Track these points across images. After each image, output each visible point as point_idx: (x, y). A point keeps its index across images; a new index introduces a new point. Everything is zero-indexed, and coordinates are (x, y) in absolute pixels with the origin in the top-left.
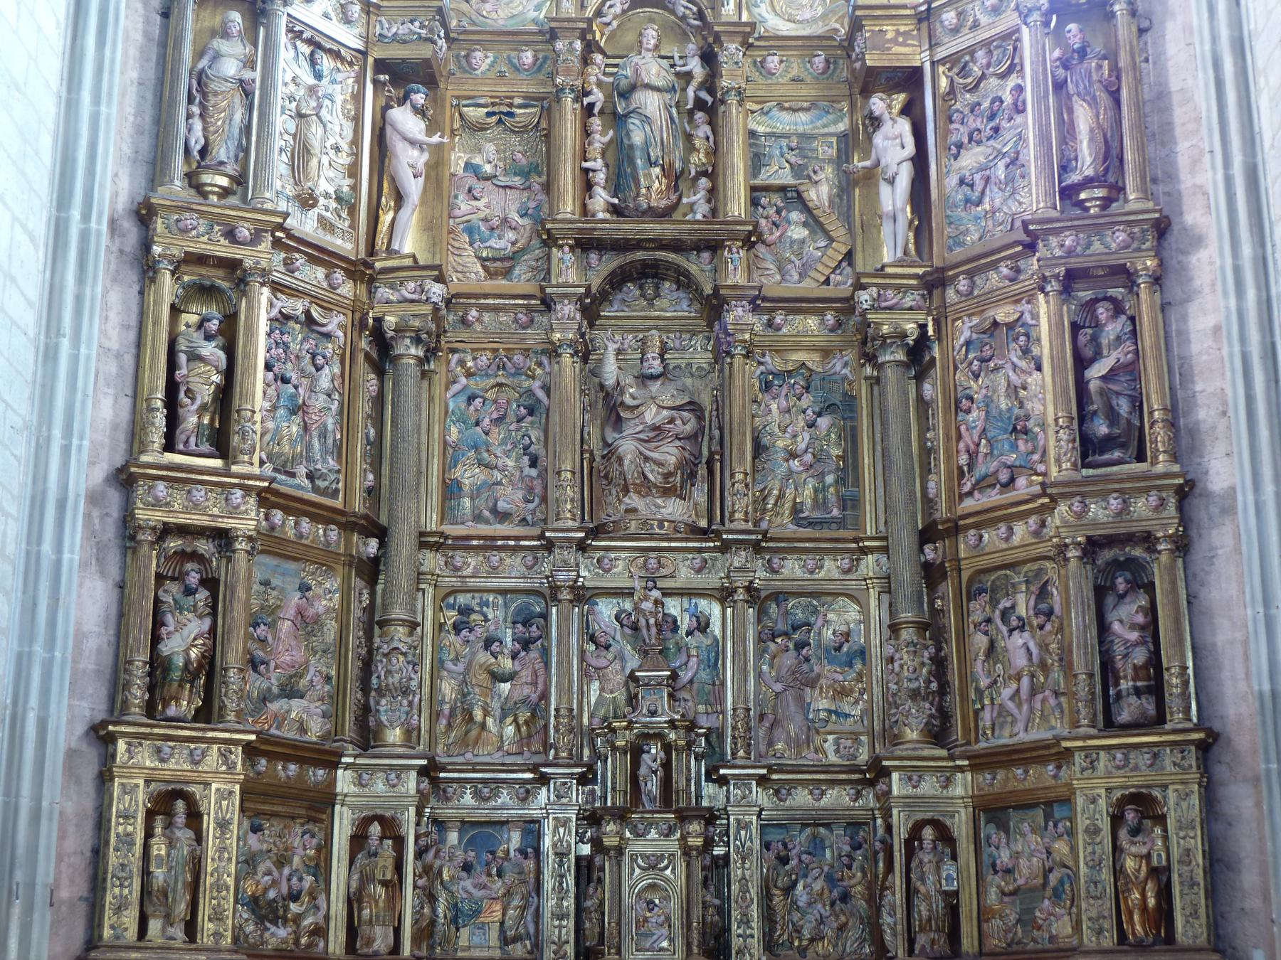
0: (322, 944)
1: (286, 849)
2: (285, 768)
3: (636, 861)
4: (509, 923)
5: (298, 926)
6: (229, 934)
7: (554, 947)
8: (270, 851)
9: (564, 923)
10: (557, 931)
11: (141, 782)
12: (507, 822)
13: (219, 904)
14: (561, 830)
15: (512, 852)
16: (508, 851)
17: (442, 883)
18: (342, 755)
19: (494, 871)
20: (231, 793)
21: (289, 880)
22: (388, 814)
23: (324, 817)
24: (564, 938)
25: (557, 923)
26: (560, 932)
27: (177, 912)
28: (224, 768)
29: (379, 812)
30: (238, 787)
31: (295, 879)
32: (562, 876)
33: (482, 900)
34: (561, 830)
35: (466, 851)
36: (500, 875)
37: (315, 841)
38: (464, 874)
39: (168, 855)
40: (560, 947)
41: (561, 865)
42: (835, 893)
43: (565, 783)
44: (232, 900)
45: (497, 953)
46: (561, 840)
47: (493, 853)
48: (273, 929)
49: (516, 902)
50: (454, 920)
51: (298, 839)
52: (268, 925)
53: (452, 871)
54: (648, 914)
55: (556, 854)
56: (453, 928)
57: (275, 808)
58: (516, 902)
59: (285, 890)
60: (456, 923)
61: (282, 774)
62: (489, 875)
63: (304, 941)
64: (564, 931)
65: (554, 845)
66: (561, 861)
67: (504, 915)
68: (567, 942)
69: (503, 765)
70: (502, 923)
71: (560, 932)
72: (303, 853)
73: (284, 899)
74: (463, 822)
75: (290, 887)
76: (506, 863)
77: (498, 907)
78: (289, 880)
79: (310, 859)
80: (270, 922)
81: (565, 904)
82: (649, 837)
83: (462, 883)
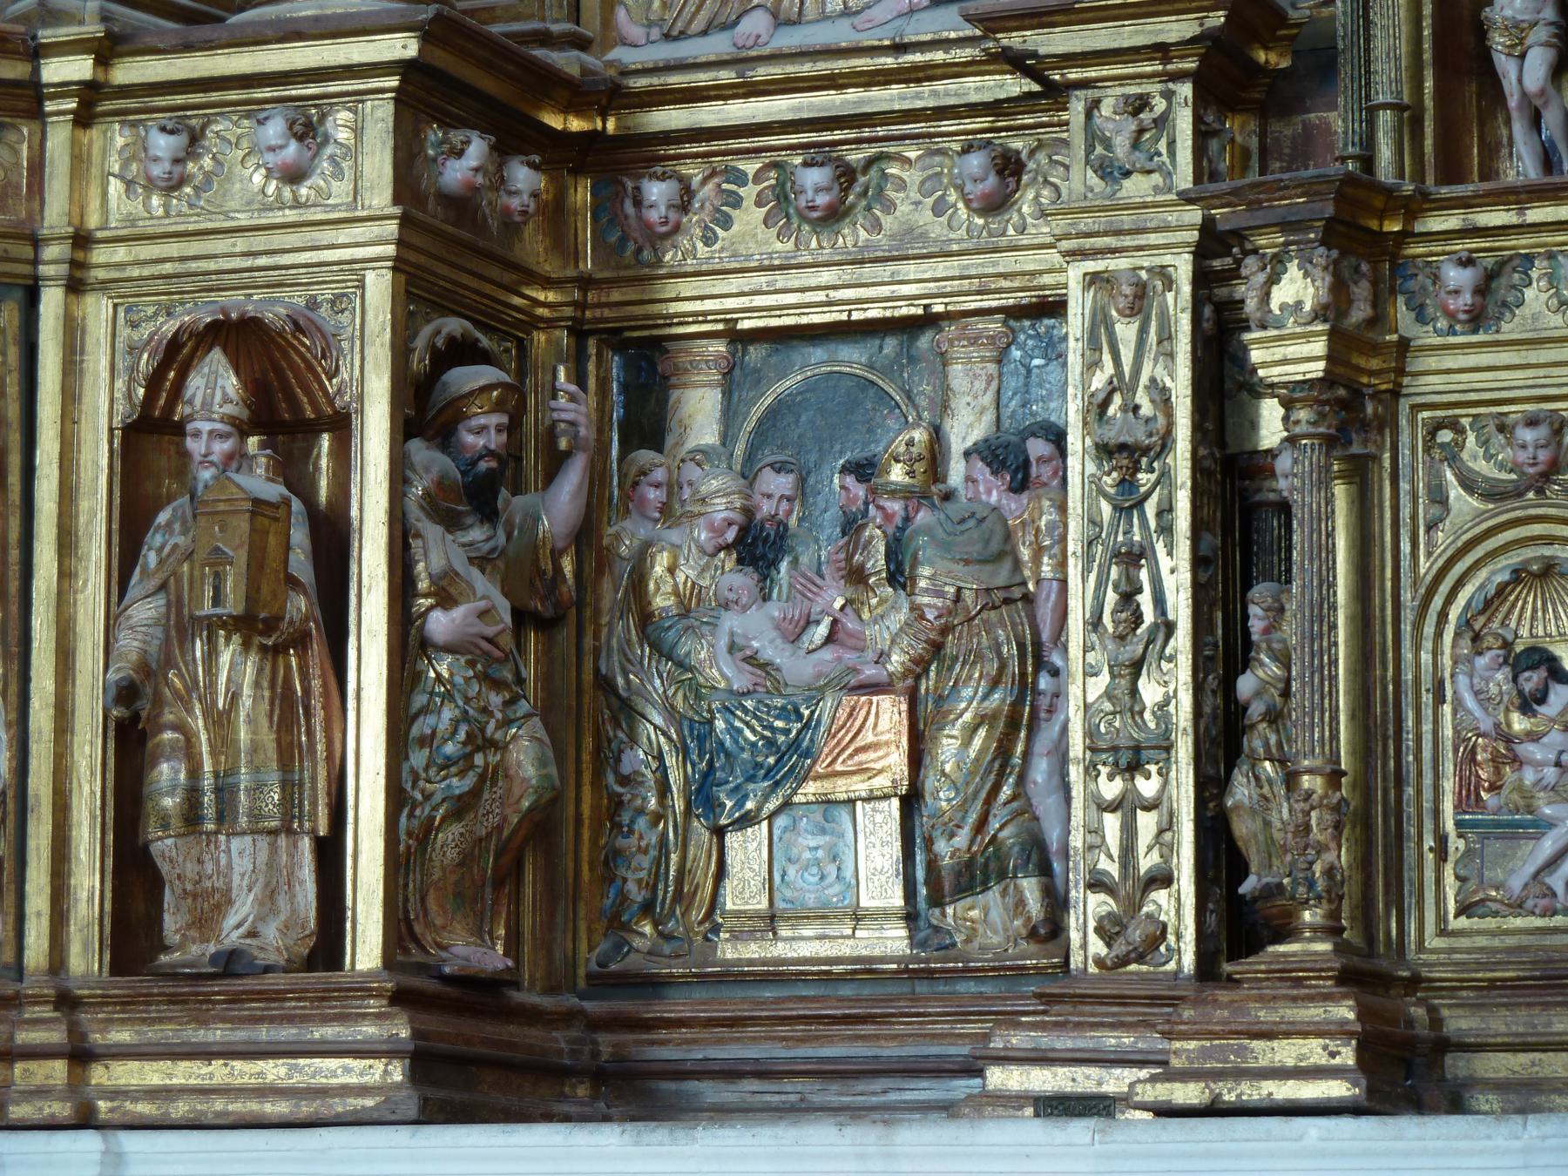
3: (1452, 456)
4: (941, 797)
7: (1099, 904)
9: (1148, 787)
10: (1112, 824)
12: (929, 321)
14: (1126, 332)
15: (956, 472)
16: (934, 458)
17: (646, 618)
18: (37, 53)
19: (877, 561)
22: (274, 308)
24: (1147, 861)
25: (1111, 789)
26: (1129, 831)
29: (236, 302)
32: (1133, 557)
33: (815, 694)
34: (1126, 332)
35: (749, 475)
36: (899, 575)
38: (741, 581)
40: (1133, 905)
41: (1129, 502)
43: (1139, 105)
45: (892, 941)
46: (1119, 385)
47: (864, 470)
49: (971, 699)
50: (702, 796)
53: (686, 573)
54: (1519, 723)
55: (1105, 451)
56: (701, 832)
58: (971, 699)
60: (712, 806)
62: (856, 576)
64: (1147, 823)
65: (1098, 408)
66: (1127, 483)
67: (917, 757)
68: (1162, 878)
69: (899, 48)
70: (911, 801)
71: (1129, 831)
74: (738, 338)
76: (923, 517)
77: (889, 715)
81: (1150, 692)
82: (1510, 329)
83: (731, 622)
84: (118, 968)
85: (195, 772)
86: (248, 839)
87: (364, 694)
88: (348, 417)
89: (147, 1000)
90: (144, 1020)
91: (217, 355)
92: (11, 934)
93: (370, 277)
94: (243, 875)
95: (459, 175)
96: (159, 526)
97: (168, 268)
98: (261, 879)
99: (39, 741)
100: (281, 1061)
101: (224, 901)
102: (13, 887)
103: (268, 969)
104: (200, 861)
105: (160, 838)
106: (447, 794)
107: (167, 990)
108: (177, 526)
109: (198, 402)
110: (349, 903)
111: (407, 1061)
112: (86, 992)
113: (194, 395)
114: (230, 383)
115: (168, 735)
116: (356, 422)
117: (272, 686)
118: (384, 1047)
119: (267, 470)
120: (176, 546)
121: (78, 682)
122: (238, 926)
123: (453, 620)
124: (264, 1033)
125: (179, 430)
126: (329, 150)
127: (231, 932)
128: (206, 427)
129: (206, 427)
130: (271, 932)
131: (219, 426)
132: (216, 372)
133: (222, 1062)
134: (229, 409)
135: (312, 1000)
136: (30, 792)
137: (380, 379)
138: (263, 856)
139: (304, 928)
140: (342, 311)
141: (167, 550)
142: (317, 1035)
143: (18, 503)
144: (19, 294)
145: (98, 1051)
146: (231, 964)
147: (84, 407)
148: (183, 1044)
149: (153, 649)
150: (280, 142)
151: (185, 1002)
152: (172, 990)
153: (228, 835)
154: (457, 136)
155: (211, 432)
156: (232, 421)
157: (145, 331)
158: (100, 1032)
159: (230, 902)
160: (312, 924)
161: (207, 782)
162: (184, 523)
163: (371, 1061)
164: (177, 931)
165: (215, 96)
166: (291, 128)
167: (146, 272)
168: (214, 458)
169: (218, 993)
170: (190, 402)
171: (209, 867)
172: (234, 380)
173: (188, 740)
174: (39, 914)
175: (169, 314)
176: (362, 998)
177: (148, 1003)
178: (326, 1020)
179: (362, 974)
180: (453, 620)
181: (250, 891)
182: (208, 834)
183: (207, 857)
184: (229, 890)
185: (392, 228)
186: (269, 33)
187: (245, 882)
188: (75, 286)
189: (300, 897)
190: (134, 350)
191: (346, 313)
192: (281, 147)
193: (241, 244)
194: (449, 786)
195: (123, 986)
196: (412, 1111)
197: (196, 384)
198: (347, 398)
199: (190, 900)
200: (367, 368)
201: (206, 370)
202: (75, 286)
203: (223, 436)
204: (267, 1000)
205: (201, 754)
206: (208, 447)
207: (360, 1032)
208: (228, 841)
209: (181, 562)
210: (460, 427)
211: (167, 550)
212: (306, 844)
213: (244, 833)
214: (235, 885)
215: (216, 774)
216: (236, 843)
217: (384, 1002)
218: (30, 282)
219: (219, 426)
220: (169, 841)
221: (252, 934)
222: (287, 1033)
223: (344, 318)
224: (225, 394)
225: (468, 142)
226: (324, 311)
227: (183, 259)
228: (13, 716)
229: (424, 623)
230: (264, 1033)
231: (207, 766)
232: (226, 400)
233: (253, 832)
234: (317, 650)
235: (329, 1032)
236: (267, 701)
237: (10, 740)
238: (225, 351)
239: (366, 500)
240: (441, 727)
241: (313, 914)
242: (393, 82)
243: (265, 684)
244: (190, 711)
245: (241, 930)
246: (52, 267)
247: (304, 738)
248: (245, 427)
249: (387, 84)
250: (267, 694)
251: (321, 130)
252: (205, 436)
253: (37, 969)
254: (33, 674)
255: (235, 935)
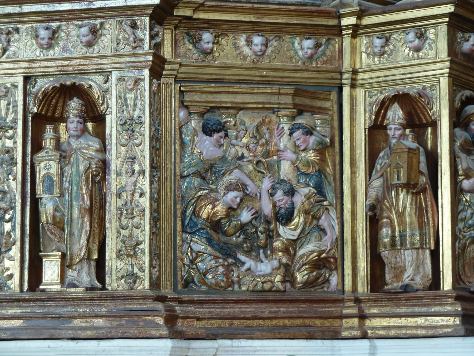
0: (334, 280)
1: (267, 154)
2: (249, 42)
5: (292, 257)
6: (146, 274)
8: (242, 157)
11: (20, 81)
13: (131, 236)
18: (340, 17)
20: (137, 81)
21: (272, 195)
22: (412, 90)
23: (327, 104)
27: (76, 248)
28: (128, 50)
29: (401, 89)
30: (146, 73)
31: (279, 195)
37: (312, 140)
39: (61, 174)
42: (11, 29)
44: (147, 228)
48: (249, 263)
51: (285, 138)
52: (243, 258)
57: (239, 99)
59: (267, 209)
61: (247, 50)
63: (300, 277)
72: (294, 157)
73: (268, 222)
75: (274, 205)
78: (272, 195)
79: (308, 164)
80: (248, 253)
84: (372, 290)
85: (393, 231)
86: (410, 251)
87: (444, 206)
88: (436, 122)
89: (382, 300)
90: (381, 306)
91: (396, 105)
92: (340, 281)
93: (442, 79)
94: (409, 262)
95: (468, 47)
96: (380, 157)
97: (381, 79)
98: (415, 263)
99: (347, 223)
100: (422, 318)
101: (404, 270)
102: (340, 267)
103: (417, 290)
104: (396, 258)
105: (384, 251)
106: (470, 236)
107: (387, 297)
108: (386, 157)
109: (391, 119)
110: (441, 269)
111: (461, 317)
112: (363, 298)
113: (389, 117)
114: (400, 113)
115: (385, 220)
116: (438, 123)
117: (416, 205)
118: (453, 313)
119: (412, 139)
120: (385, 163)
121: (358, 205)
122: (408, 277)
123: (470, 183)
124: (417, 310)
125: (385, 128)
126: (428, 41)
127: (406, 279)
128: (393, 127)
129: (393, 127)
130: (418, 279)
131: (397, 126)
132: (396, 110)
133: (404, 318)
134: (400, 121)
135: (431, 299)
136: (345, 238)
137: (445, 110)
138: (415, 256)
139: (428, 278)
140: (433, 90)
141: (383, 164)
142: (433, 310)
143: (338, 151)
144: (336, 89)
145: (368, 315)
146: (406, 289)
147: (357, 122)
148: (393, 313)
149: (380, 194)
150: (413, 40)
151: (393, 300)
152: (389, 297)
153: (404, 250)
154: (467, 35)
155: (395, 128)
156: (401, 124)
157: (374, 99)
158: (368, 310)
159: (405, 270)
160: (430, 276)
161: (397, 234)
162: (388, 156)
163: (450, 318)
164: (390, 279)
165: (393, 27)
166: (416, 35)
167: (374, 81)
168: (396, 136)
169: (403, 298)
170: (388, 119)
171: (399, 260)
172: (401, 112)
173: (391, 221)
174: (348, 275)
175: (381, 93)
176: (446, 298)
177: (382, 301)
178: (436, 305)
179: (446, 291)
180: (470, 183)
181: (411, 266)
182: (398, 249)
183: (398, 257)
184: (405, 266)
185: (448, 64)
186: (409, 7)
187: (410, 264)
188: (353, 86)
189: (426, 268)
190: (371, 104)
191: (435, 91)
192: (414, 41)
193: (402, 71)
194: (471, 234)
195: (374, 296)
196: (463, 332)
197: (390, 114)
198: (436, 116)
199: (393, 270)
200: (442, 107)
201: (393, 109)
202: (353, 86)
203: (399, 129)
204: (417, 299)
205: (395, 225)
206: (394, 133)
207: (446, 309)
208: (404, 252)
209: (387, 168)
210: (470, 124)
211: (383, 164)
212: (428, 252)
213: (409, 249)
214: (407, 265)
215: (400, 232)
216: (406, 252)
217: (453, 300)
218: (340, 85)
219: (397, 126)
220: (387, 252)
221: (412, 280)
222: (424, 309)
223: (434, 92)
224: (399, 117)
225: (470, 37)
226: (428, 90)
227: (385, 76)
228: (339, 215)
229: (461, 184)
230: (417, 310)
231: (397, 229)
232: (399, 118)
233: (412, 249)
234: (429, 193)
235: (437, 309)
236: (414, 209)
237: (338, 223)
238: (398, 103)
239: (442, 147)
240: (468, 215)
241: (430, 273)
242: (447, 19)
243: (414, 204)
244: (391, 213)
245: (409, 278)
246: (346, 81)
247: (426, 220)
248: (405, 126)
249: (445, 20)
250: (414, 207)
251: (425, 35)
252: (393, 129)
253: (348, 291)
254: (344, 203)
255: (407, 280)
